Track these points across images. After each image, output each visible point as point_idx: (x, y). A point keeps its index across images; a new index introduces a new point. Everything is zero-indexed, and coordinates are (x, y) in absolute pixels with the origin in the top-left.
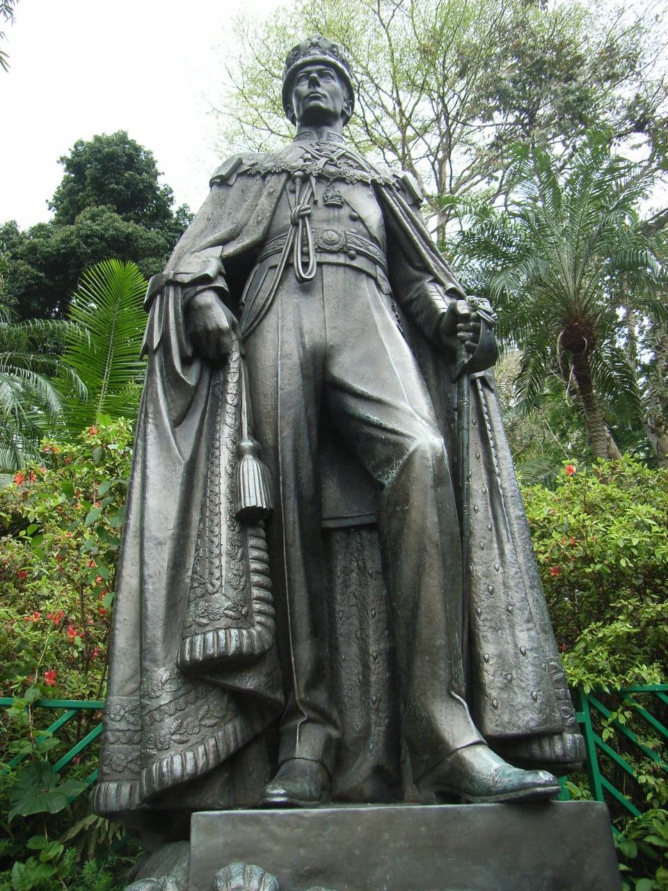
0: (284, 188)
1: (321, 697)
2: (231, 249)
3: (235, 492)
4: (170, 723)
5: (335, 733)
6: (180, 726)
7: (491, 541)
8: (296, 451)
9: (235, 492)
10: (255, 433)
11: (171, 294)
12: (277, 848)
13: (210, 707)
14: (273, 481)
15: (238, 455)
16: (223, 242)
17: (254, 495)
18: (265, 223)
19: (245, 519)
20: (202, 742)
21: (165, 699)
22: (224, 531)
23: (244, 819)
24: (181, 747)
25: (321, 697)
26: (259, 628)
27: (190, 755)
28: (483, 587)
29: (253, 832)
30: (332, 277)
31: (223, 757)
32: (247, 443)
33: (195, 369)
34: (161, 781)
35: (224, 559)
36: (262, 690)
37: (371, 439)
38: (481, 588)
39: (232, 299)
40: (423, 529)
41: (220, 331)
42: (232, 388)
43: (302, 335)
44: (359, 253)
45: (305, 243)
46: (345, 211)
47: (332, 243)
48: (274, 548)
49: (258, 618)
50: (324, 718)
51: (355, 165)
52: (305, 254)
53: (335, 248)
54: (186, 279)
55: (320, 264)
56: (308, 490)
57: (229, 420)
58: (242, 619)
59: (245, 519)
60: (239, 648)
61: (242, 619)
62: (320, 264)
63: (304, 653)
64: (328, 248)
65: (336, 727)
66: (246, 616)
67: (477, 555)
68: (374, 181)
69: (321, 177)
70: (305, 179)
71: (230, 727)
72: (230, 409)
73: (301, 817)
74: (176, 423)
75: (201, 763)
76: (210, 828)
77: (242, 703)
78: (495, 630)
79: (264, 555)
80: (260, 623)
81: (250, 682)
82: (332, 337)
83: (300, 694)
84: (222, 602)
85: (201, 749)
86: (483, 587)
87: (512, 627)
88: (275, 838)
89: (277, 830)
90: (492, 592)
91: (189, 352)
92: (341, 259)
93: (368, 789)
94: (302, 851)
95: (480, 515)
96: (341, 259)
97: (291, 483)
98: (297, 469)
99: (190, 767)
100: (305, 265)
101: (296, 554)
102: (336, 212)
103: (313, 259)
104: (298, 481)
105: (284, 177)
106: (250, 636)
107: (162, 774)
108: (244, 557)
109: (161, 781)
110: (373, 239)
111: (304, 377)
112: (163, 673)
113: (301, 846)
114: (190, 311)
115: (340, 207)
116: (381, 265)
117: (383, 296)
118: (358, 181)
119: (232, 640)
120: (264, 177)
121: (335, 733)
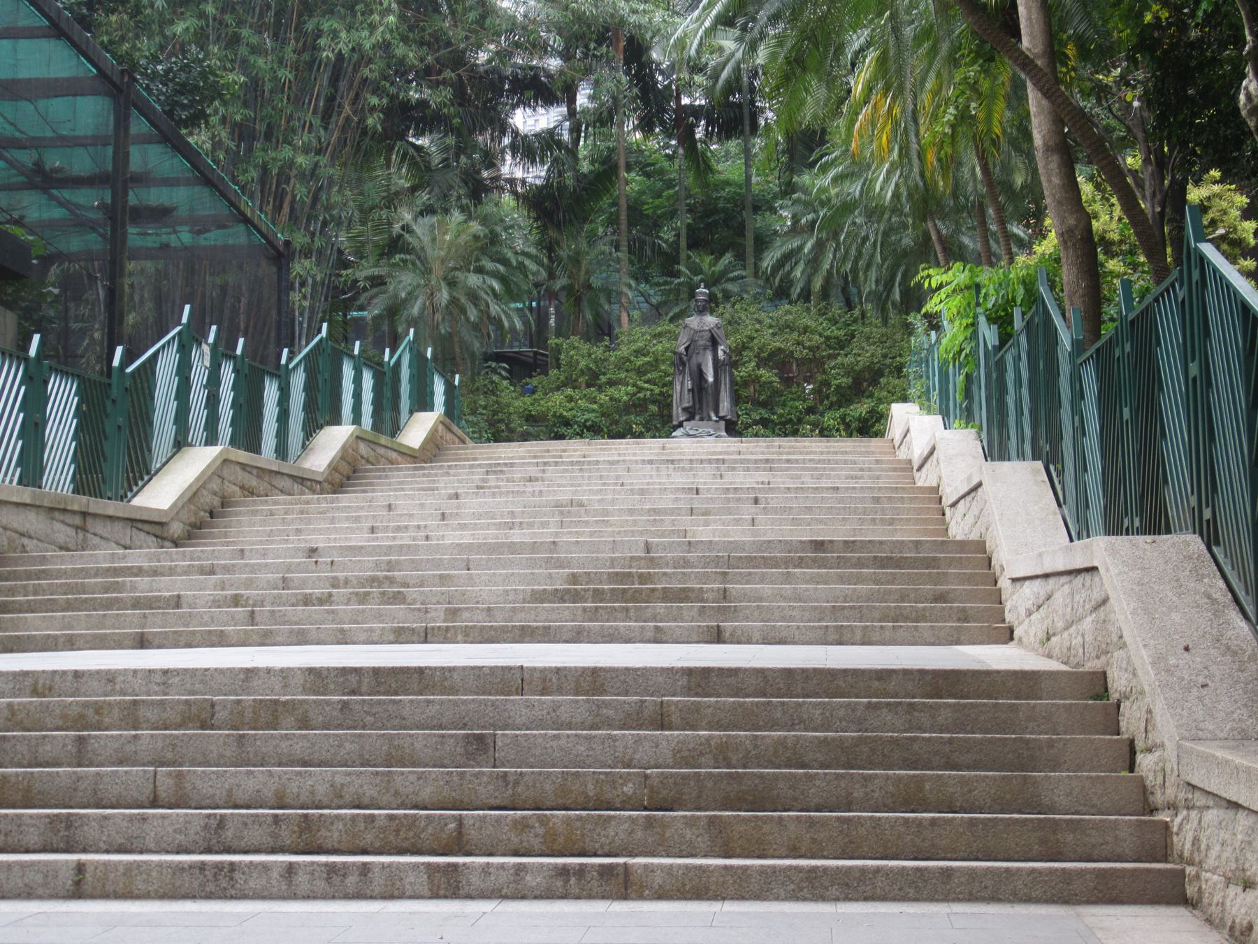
14: (693, 384)
30: (701, 352)
59: (689, 390)
63: (697, 406)
77: (690, 413)
114: (681, 359)
119: (686, 405)
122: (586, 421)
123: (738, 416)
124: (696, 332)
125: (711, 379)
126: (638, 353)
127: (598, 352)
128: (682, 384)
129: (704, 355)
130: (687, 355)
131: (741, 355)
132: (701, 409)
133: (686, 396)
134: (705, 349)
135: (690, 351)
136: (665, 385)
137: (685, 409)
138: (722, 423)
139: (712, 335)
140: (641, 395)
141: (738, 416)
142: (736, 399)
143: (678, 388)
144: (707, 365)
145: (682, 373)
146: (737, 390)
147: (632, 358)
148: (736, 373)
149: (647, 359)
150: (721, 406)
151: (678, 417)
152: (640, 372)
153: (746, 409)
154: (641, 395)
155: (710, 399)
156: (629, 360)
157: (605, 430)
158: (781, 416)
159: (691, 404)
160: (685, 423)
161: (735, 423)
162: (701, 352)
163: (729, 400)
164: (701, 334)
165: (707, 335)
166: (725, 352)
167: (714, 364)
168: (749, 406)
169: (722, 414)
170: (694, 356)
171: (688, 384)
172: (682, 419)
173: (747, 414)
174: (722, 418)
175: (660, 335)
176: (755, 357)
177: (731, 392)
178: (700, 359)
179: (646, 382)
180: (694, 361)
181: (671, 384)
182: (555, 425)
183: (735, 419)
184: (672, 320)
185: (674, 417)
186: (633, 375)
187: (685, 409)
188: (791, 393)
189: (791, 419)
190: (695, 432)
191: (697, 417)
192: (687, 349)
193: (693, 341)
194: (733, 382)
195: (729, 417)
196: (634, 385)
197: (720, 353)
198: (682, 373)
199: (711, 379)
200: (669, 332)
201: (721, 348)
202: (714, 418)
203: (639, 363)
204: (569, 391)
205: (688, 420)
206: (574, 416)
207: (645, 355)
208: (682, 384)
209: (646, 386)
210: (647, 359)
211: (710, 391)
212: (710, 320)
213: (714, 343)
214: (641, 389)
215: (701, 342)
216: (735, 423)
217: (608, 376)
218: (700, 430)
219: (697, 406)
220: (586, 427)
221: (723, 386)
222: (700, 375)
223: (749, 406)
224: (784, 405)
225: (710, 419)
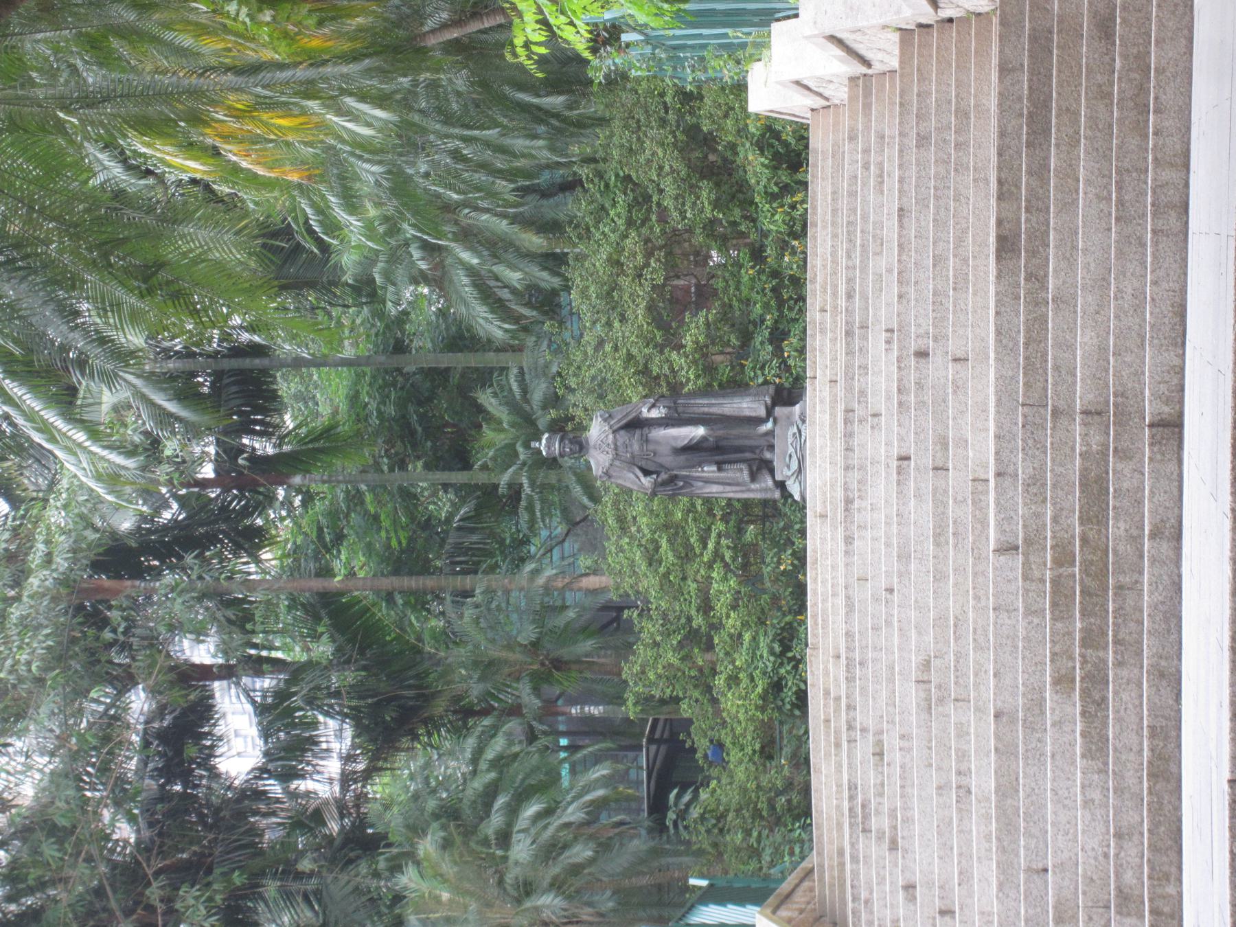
2: (640, 474)
10: (693, 467)
14: (709, 463)
15: (703, 471)
17: (714, 468)
19: (720, 469)
22: (722, 474)
30: (651, 447)
48: (725, 462)
58: (741, 470)
59: (720, 469)
61: (741, 470)
63: (748, 455)
77: (759, 469)
81: (755, 468)
84: (738, 475)
101: (726, 457)
112: (753, 486)
114: (664, 484)
119: (746, 474)
122: (772, 652)
123: (766, 382)
124: (617, 456)
125: (700, 431)
126: (652, 558)
127: (649, 629)
128: (708, 481)
129: (657, 442)
130: (658, 473)
131: (657, 377)
132: (752, 449)
133: (730, 474)
134: (647, 441)
135: (651, 467)
136: (710, 512)
137: (753, 477)
138: (779, 411)
139: (622, 428)
140: (728, 555)
141: (766, 382)
142: (737, 386)
143: (714, 489)
144: (675, 438)
145: (688, 481)
146: (720, 385)
147: (662, 570)
148: (690, 386)
149: (664, 544)
150: (747, 413)
151: (766, 490)
152: (687, 555)
153: (754, 369)
154: (728, 555)
155: (735, 432)
156: (668, 573)
157: (789, 618)
158: (766, 306)
159: (744, 467)
160: (779, 477)
161: (779, 389)
162: (651, 447)
163: (736, 400)
164: (621, 449)
165: (623, 436)
166: (653, 406)
167: (673, 426)
168: (748, 364)
169: (762, 412)
170: (660, 460)
171: (709, 470)
172: (770, 483)
173: (762, 368)
174: (770, 412)
175: (621, 520)
176: (661, 352)
177: (723, 396)
178: (664, 450)
179: (705, 546)
180: (668, 460)
181: (708, 502)
182: (779, 709)
183: (771, 389)
184: (595, 499)
185: (768, 496)
186: (691, 569)
187: (753, 477)
188: (727, 287)
189: (773, 290)
190: (794, 458)
191: (768, 455)
192: (646, 473)
193: (632, 463)
194: (706, 391)
196: (710, 566)
197: (655, 414)
198: (688, 481)
199: (700, 431)
200: (616, 504)
201: (646, 413)
202: (769, 425)
203: (671, 558)
204: (720, 682)
205: (772, 472)
206: (765, 673)
207: (657, 548)
208: (708, 481)
209: (711, 546)
210: (664, 544)
211: (720, 433)
212: (597, 431)
213: (636, 425)
214: (717, 555)
215: (636, 447)
216: (779, 389)
217: (693, 612)
218: (791, 450)
219: (748, 455)
220: (782, 654)
221: (714, 410)
222: (692, 449)
224: (748, 302)
225: (771, 433)
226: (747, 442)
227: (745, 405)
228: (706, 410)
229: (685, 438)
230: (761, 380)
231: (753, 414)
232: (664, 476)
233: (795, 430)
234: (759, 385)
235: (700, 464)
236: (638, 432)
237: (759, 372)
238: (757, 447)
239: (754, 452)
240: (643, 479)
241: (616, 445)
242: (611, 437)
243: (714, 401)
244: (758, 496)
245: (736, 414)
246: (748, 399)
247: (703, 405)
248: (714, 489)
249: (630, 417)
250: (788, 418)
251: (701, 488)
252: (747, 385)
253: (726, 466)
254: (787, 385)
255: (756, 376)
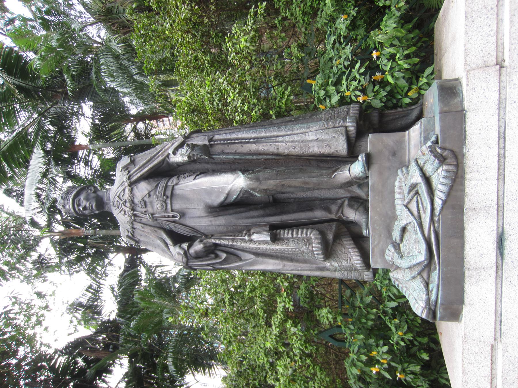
0: (139, 222)
1: (334, 208)
2: (169, 242)
3: (265, 243)
4: (344, 263)
5: (346, 203)
6: (345, 260)
7: (276, 145)
8: (247, 218)
9: (265, 243)
11: (191, 263)
12: (381, 243)
13: (339, 249)
15: (251, 241)
16: (167, 245)
17: (266, 237)
18: (156, 229)
19: (275, 239)
20: (350, 253)
21: (336, 265)
22: (279, 247)
23: (373, 252)
24: (352, 260)
25: (334, 208)
26: (312, 235)
27: (354, 258)
28: (293, 150)
29: (377, 250)
30: (177, 206)
31: (354, 246)
32: (246, 238)
33: (219, 253)
34: (363, 267)
35: (289, 248)
36: (332, 233)
37: (242, 197)
38: (293, 151)
39: (191, 240)
40: (276, 185)
41: (205, 247)
42: (225, 242)
43: (202, 217)
44: (164, 194)
45: (165, 217)
46: (146, 199)
47: (162, 206)
49: (308, 235)
50: (341, 206)
51: (122, 193)
52: (169, 217)
53: (164, 205)
54: (185, 260)
55: (172, 211)
56: (261, 212)
57: (239, 244)
58: (309, 241)
59: (275, 239)
60: (319, 243)
62: (172, 211)
63: (319, 214)
64: (165, 207)
65: (344, 201)
66: (308, 240)
67: (281, 151)
68: (130, 186)
69: (133, 209)
70: (135, 215)
71: (345, 243)
72: (234, 243)
73: (372, 235)
74: (240, 259)
75: (356, 254)
76: (376, 262)
77: (337, 237)
78: (309, 148)
79: (286, 231)
80: (310, 235)
81: (330, 236)
82: (201, 206)
83: (333, 216)
85: (352, 254)
86: (293, 150)
87: (307, 141)
88: (378, 244)
89: (376, 243)
90: (295, 147)
91: (213, 256)
92: (169, 202)
93: (366, 190)
94: (382, 236)
95: (266, 148)
96: (169, 202)
97: (259, 220)
98: (253, 217)
99: (358, 258)
100: (173, 217)
102: (148, 203)
103: (171, 214)
104: (258, 217)
105: (134, 223)
106: (315, 239)
107: (361, 266)
108: (288, 239)
109: (363, 267)
110: (157, 186)
111: (219, 216)
112: (328, 264)
113: (381, 235)
114: (198, 256)
115: (145, 202)
116: (167, 183)
117: (180, 183)
118: (131, 193)
119: (316, 246)
120: (134, 229)
121: (346, 203)
123: (343, 101)
129: (184, 198)
139: (146, 177)
141: (343, 101)
144: (209, 192)
146: (279, 115)
150: (316, 149)
163: (298, 129)
164: (140, 210)
165: (143, 188)
167: (204, 172)
173: (337, 83)
177: (279, 125)
183: (353, 110)
185: (353, 276)
191: (351, 215)
195: (351, 125)
211: (271, 184)
215: (157, 206)
221: (262, 147)
223: (316, 83)
226: (317, 194)
227: (312, 136)
228: (253, 147)
229: (220, 191)
230: (335, 99)
231: (326, 150)
232: (198, 247)
233: (417, 178)
234: (333, 107)
235: (248, 230)
236: (162, 184)
237: (332, 89)
238: (334, 200)
239: (328, 210)
240: (171, 248)
241: (132, 202)
242: (127, 191)
243: (263, 134)
244: (338, 275)
245: (298, 151)
246: (316, 126)
247: (248, 141)
248: (270, 265)
249: (155, 162)
250: (394, 154)
251: (252, 264)
252: (316, 108)
253: (285, 234)
254: (377, 104)
255: (328, 95)
